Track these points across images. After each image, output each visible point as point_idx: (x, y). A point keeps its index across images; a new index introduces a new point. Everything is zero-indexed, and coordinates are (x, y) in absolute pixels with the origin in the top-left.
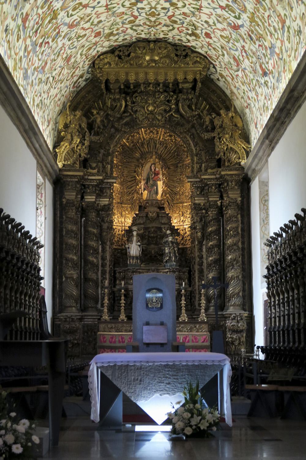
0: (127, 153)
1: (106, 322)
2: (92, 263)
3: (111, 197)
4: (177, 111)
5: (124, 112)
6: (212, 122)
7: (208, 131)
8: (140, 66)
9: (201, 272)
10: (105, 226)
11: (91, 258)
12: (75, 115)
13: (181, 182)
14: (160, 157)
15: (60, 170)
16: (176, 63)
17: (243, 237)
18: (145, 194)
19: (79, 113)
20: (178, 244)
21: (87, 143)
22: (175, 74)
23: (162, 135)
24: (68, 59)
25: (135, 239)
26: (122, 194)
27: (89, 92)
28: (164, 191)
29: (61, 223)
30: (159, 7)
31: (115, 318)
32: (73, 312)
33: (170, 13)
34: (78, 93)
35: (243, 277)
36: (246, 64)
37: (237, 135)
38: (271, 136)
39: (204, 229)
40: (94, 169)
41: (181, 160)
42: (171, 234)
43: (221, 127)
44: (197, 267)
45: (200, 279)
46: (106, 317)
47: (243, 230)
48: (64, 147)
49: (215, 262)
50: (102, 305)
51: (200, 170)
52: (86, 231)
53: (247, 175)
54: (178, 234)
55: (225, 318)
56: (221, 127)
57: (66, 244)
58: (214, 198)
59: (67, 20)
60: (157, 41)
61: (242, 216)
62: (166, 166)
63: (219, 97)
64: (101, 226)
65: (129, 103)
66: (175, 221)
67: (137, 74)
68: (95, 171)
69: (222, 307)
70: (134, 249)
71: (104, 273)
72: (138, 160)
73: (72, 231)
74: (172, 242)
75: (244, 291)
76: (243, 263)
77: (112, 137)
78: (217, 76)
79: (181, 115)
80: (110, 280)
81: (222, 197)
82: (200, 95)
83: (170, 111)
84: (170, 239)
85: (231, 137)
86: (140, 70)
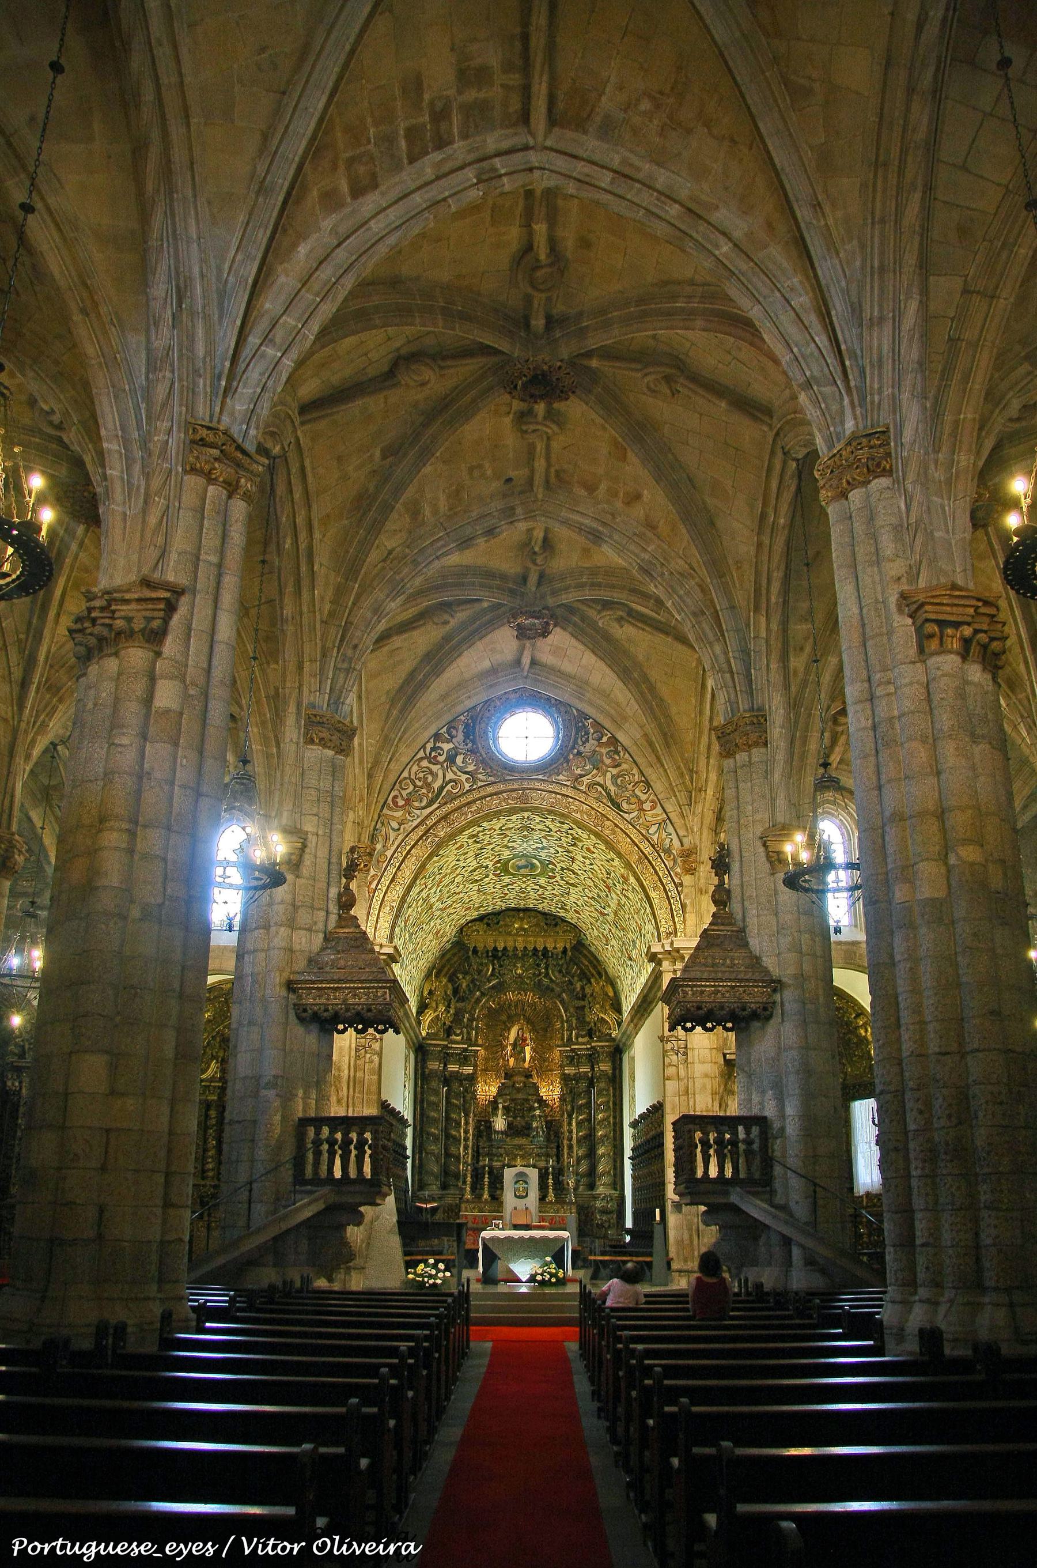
0: (492, 1015)
1: (468, 1201)
2: (454, 1137)
3: (475, 1066)
4: (547, 975)
5: (492, 975)
7: (579, 999)
8: (509, 934)
9: (570, 1147)
10: (468, 1096)
12: (441, 982)
13: (550, 1049)
14: (528, 1021)
15: (424, 1039)
16: (545, 931)
17: (614, 1112)
18: (512, 1062)
19: (445, 980)
20: (546, 1117)
21: (452, 1011)
22: (545, 942)
23: (530, 997)
24: (437, 933)
25: (500, 1111)
26: (486, 1060)
27: (454, 955)
28: (531, 1057)
29: (422, 1093)
30: (529, 888)
32: (434, 1189)
33: (540, 892)
34: (443, 956)
35: (614, 1153)
36: (613, 942)
38: (635, 1021)
39: (573, 1101)
40: (458, 1035)
41: (551, 1024)
42: (539, 1108)
43: (592, 995)
44: (566, 1142)
45: (570, 1156)
46: (468, 1196)
47: (615, 1104)
48: (428, 1017)
49: (585, 1137)
50: (464, 1183)
51: (570, 1038)
52: (448, 1102)
53: (618, 1046)
54: (547, 1105)
55: (595, 1198)
56: (592, 995)
57: (428, 1117)
59: (441, 906)
60: (527, 910)
61: (614, 1089)
62: (533, 1030)
64: (464, 1097)
65: (497, 966)
66: (544, 1090)
67: (505, 942)
68: (460, 1038)
69: (592, 1186)
70: (500, 1123)
71: (466, 1147)
72: (504, 1023)
73: (434, 1103)
74: (540, 1116)
75: (615, 1168)
76: (615, 1139)
77: (478, 1000)
78: (588, 942)
79: (551, 979)
80: (473, 1156)
81: (593, 1069)
82: (571, 960)
83: (540, 975)
84: (538, 1112)
85: (602, 1007)
86: (510, 938)
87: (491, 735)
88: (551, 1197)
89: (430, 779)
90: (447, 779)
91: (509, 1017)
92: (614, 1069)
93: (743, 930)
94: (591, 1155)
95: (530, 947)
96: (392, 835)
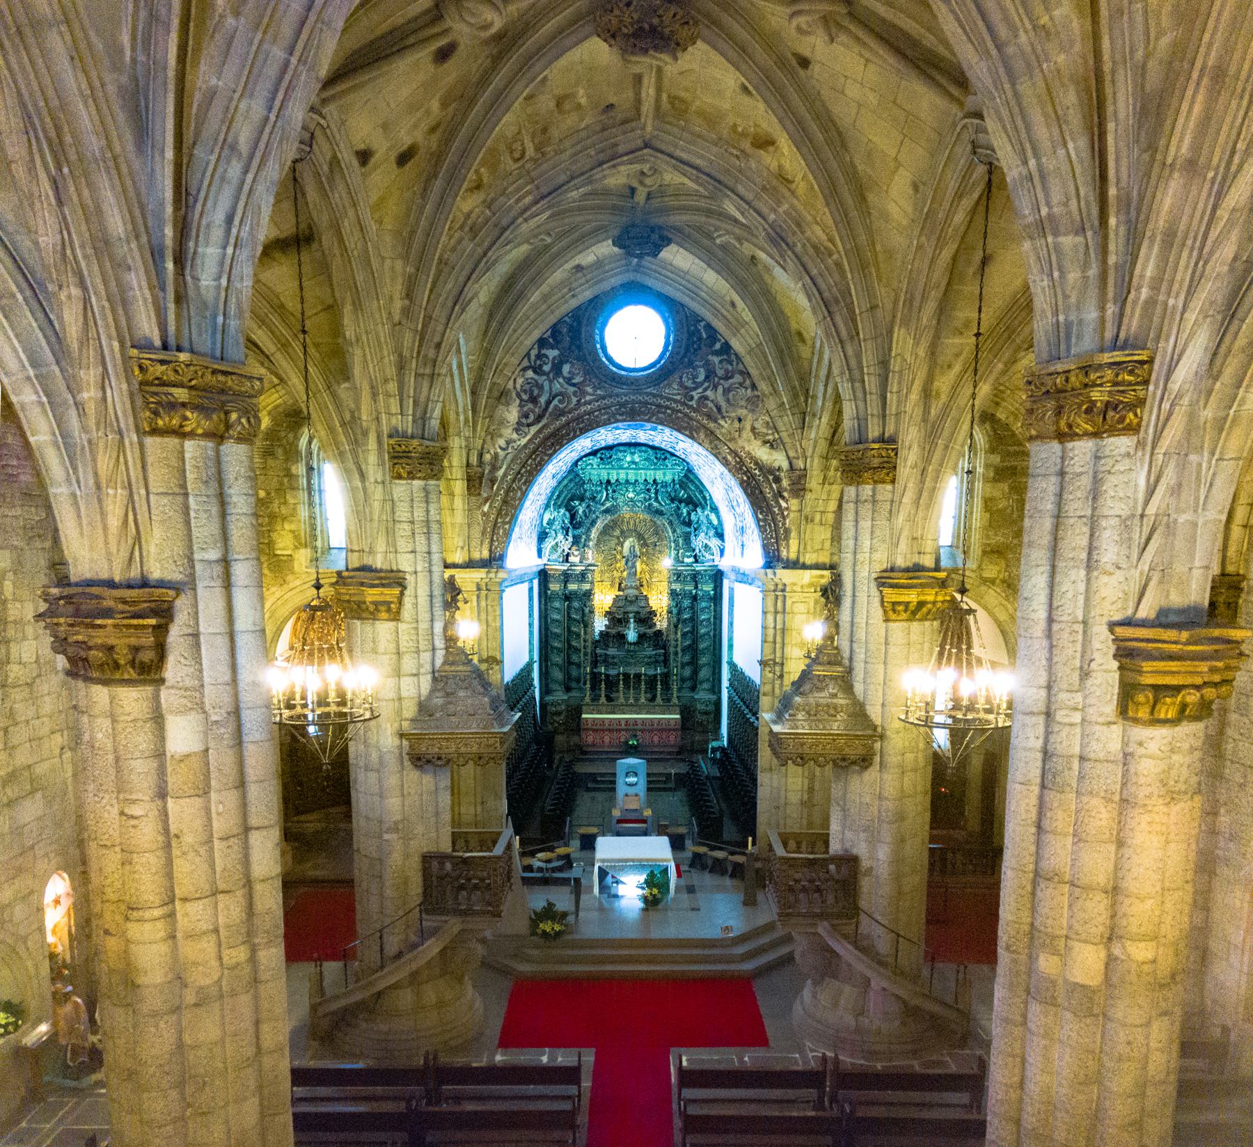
1: (587, 704)
3: (592, 583)
4: (656, 500)
6: (689, 514)
10: (587, 610)
11: (574, 643)
27: (571, 481)
31: (595, 699)
37: (712, 532)
39: (679, 613)
46: (587, 699)
58: (689, 588)
63: (697, 487)
71: (585, 654)
81: (696, 587)
87: (597, 338)
88: (659, 700)
91: (622, 532)
92: (715, 589)
93: (850, 670)
94: (694, 663)
95: (641, 480)
96: (502, 453)
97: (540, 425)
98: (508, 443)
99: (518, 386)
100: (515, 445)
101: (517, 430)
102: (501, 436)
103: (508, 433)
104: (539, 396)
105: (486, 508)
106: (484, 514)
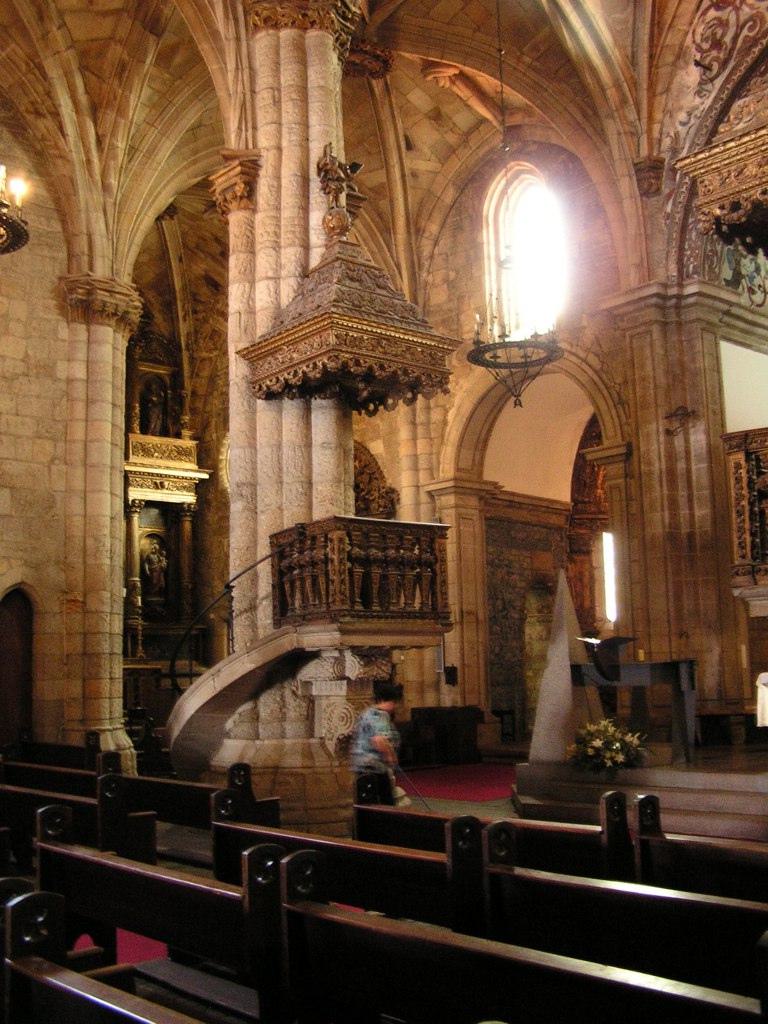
89: (719, 32)
90: (742, 19)
97: (727, 72)
98: (689, 114)
99: (698, 38)
100: (697, 113)
101: (698, 93)
102: (681, 109)
103: (691, 100)
104: (723, 35)
105: (669, 208)
106: (668, 216)
